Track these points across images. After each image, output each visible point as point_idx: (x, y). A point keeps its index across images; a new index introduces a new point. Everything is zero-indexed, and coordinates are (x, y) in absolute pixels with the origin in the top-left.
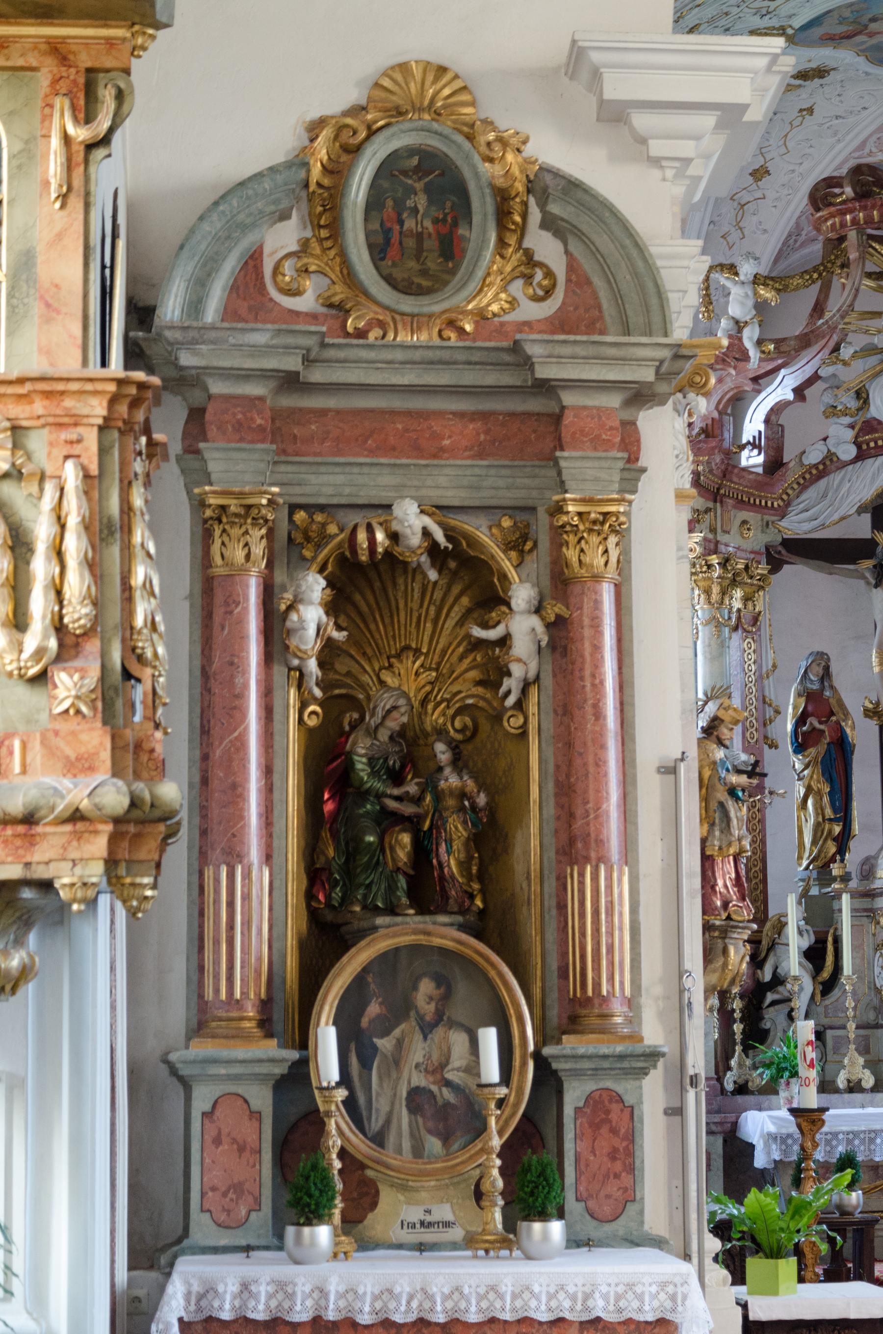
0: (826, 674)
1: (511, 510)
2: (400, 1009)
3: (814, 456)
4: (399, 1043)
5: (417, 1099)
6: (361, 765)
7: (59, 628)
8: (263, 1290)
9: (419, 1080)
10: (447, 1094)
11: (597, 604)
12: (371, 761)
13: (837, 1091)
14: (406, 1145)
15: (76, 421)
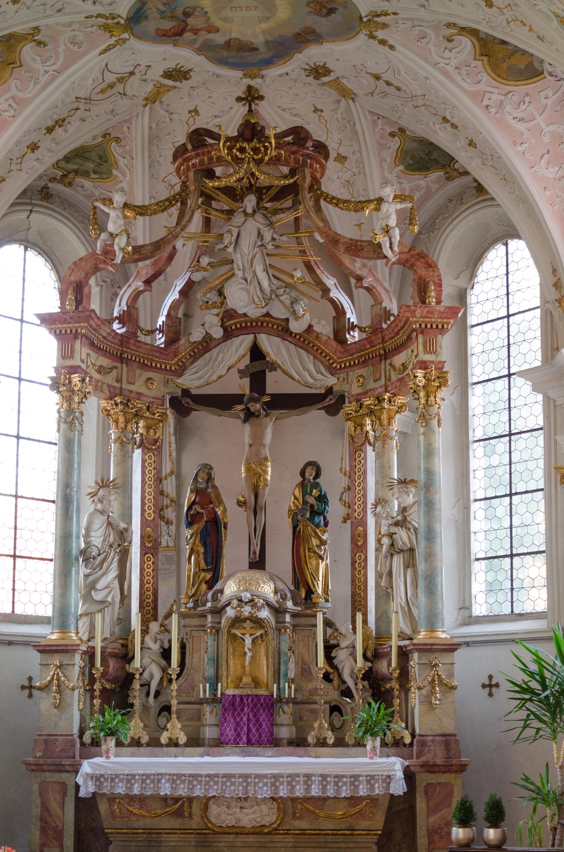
0: (210, 479)
13: (161, 745)
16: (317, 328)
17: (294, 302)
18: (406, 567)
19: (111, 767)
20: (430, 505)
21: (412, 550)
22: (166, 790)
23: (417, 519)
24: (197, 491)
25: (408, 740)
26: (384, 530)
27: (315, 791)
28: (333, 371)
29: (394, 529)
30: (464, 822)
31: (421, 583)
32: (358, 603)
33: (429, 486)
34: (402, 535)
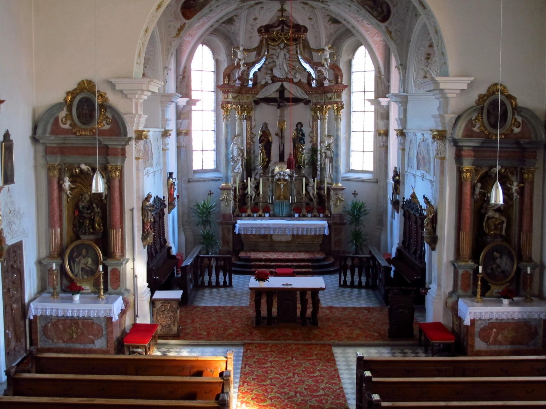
0: (267, 127)
3: (263, 82)
4: (80, 260)
5: (83, 269)
9: (83, 266)
10: (88, 268)
14: (81, 277)
16: (302, 81)
17: (295, 73)
18: (330, 162)
19: (243, 224)
20: (337, 146)
21: (332, 158)
22: (262, 233)
25: (329, 215)
28: (307, 94)
29: (326, 151)
33: (337, 140)
34: (329, 153)
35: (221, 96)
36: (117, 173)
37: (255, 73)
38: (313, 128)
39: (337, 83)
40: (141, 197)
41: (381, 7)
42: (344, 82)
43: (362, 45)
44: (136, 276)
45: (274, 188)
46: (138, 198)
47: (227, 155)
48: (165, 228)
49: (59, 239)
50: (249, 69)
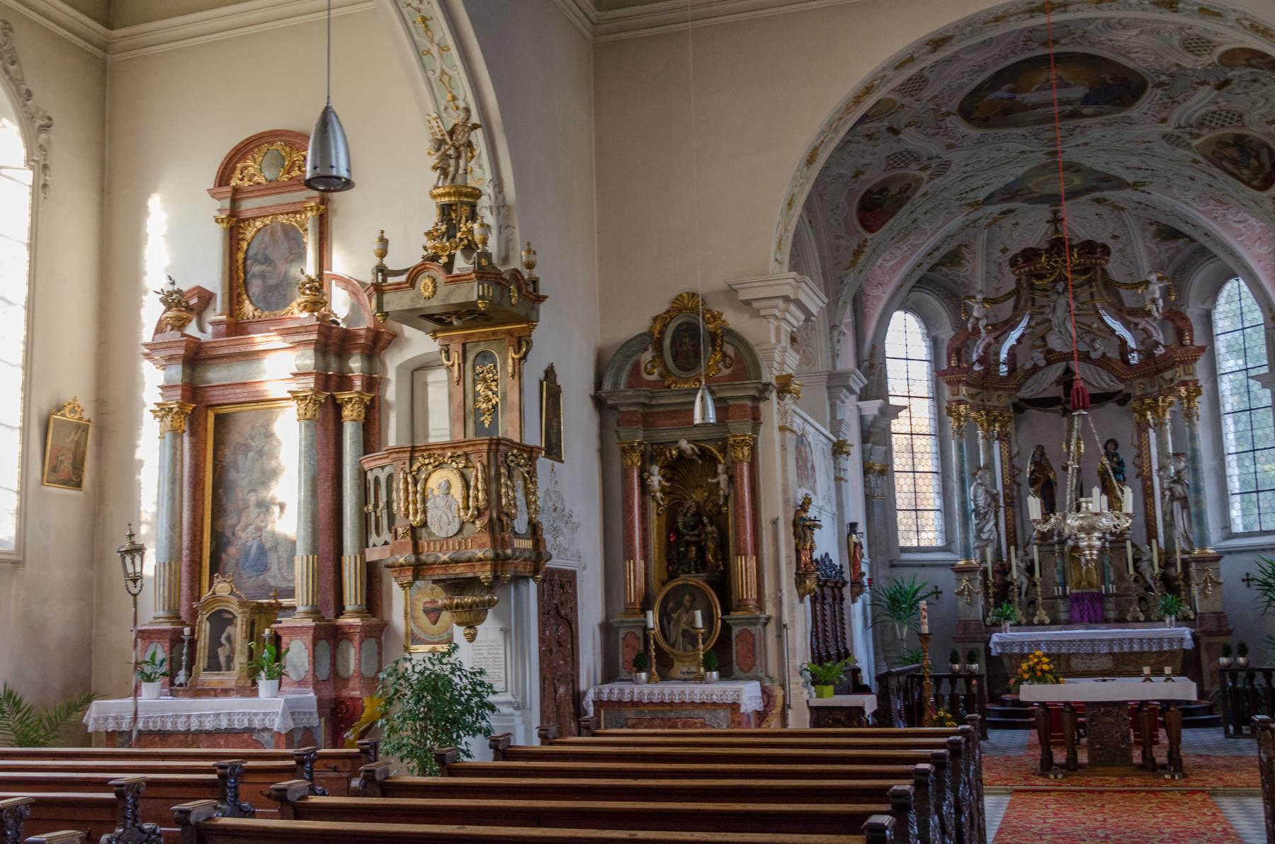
0: (1043, 454)
1: (719, 440)
2: (679, 605)
3: (1028, 366)
6: (680, 525)
7: (478, 509)
8: (616, 691)
9: (685, 627)
11: (742, 470)
12: (684, 524)
15: (480, 451)
16: (1109, 355)
17: (1093, 340)
18: (1183, 508)
19: (1005, 637)
20: (1195, 471)
21: (1186, 498)
23: (1188, 478)
24: (1034, 463)
26: (1166, 486)
27: (1136, 648)
28: (1122, 381)
30: (1226, 655)
31: (1193, 519)
32: (1151, 533)
33: (1194, 460)
34: (1178, 489)
35: (946, 391)
36: (746, 450)
37: (1012, 348)
38: (1140, 447)
39: (1182, 345)
40: (792, 503)
41: (1257, 158)
42: (1199, 341)
43: (1233, 275)
44: (789, 707)
45: (1067, 566)
46: (786, 501)
47: (964, 503)
48: (847, 631)
49: (643, 580)
50: (999, 340)
